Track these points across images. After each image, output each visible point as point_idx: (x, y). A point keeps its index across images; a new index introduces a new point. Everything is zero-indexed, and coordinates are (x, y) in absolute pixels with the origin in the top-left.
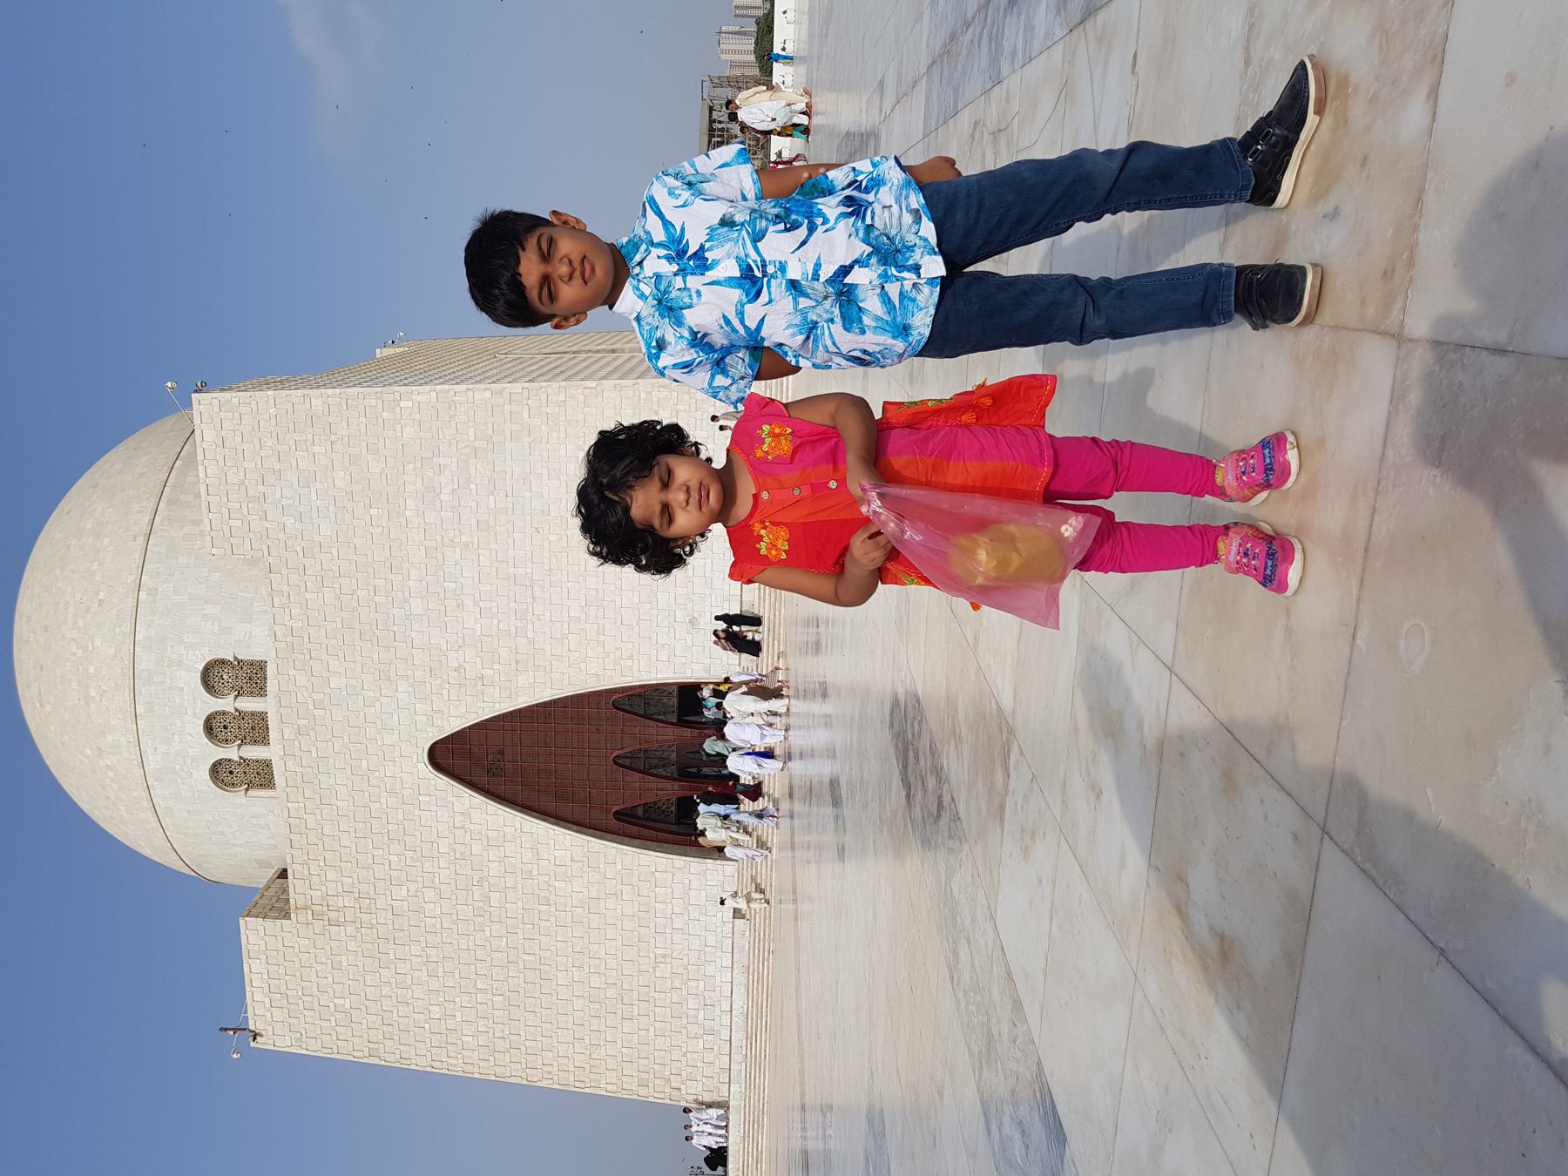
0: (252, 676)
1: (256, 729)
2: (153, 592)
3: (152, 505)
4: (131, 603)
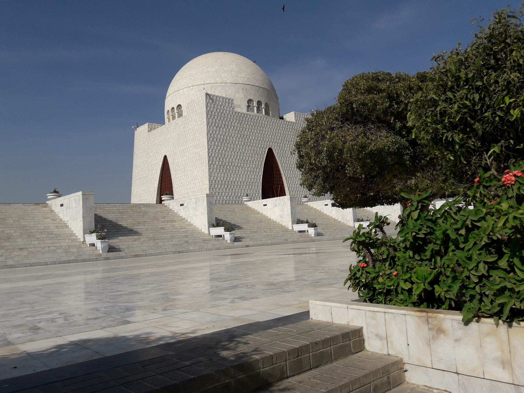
0: (180, 115)
1: (174, 118)
2: (192, 89)
3: (211, 82)
4: (190, 85)
